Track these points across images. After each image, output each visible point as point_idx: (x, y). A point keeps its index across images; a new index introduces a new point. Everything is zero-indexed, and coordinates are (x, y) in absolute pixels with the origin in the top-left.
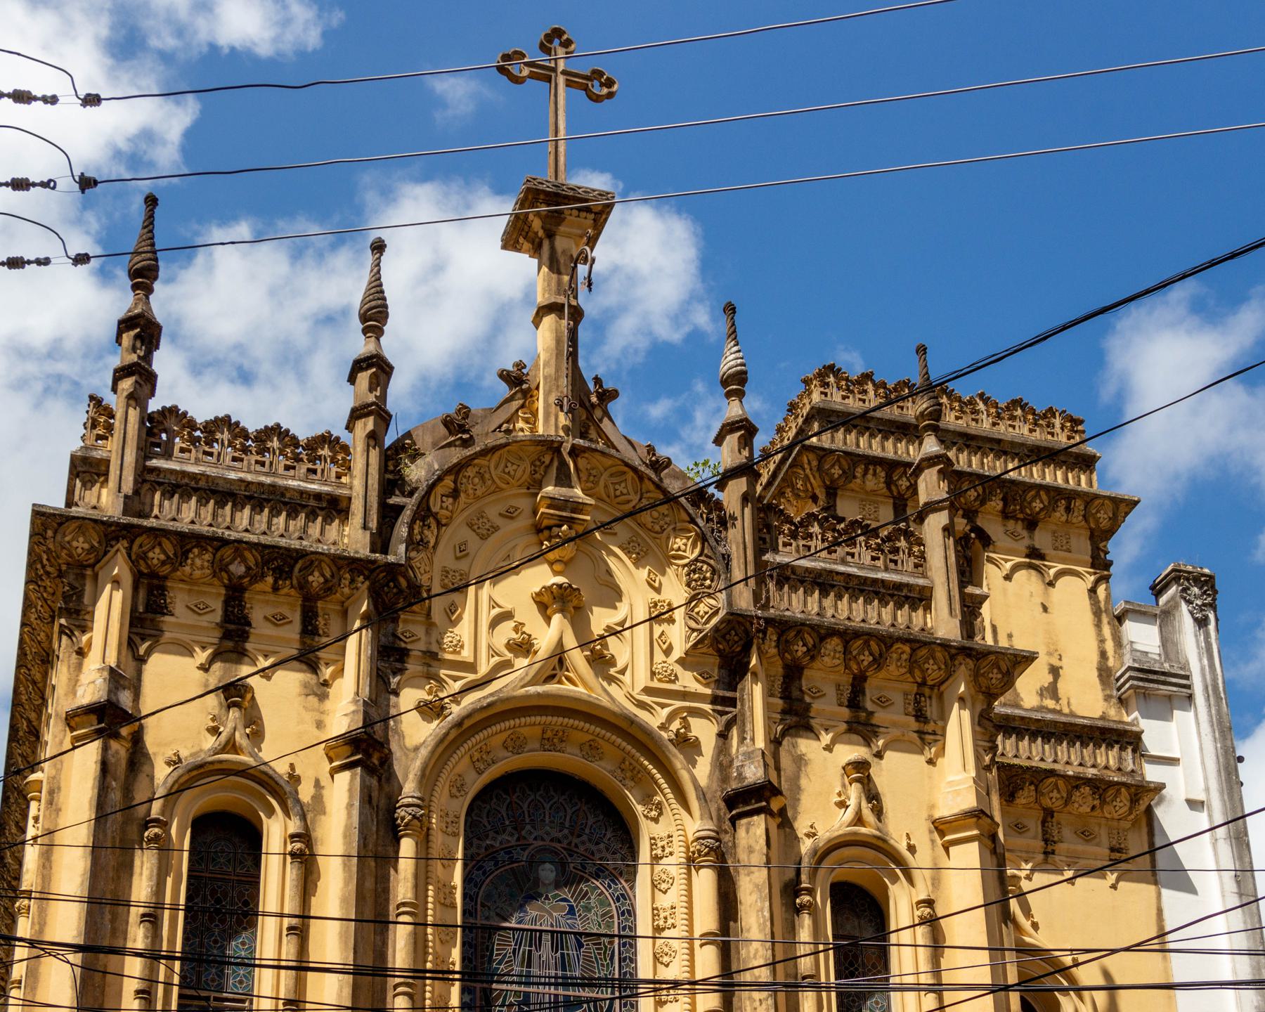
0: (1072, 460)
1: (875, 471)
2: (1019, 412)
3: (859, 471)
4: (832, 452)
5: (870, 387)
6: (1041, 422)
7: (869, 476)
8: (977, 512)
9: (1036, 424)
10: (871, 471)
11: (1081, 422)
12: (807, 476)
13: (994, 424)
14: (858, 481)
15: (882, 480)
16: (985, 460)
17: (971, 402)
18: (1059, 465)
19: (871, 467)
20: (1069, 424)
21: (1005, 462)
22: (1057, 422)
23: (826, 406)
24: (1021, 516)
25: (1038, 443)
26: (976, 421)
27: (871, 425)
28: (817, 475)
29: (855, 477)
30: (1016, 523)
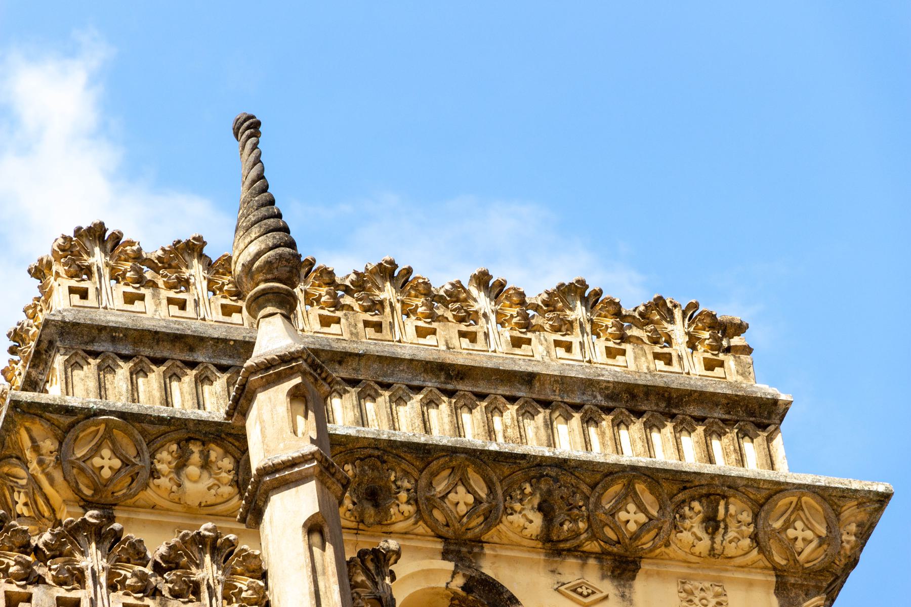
0: (719, 414)
1: (205, 456)
2: (579, 312)
3: (165, 459)
4: (89, 414)
5: (196, 271)
6: (635, 332)
7: (193, 470)
8: (479, 542)
9: (624, 338)
10: (196, 457)
11: (740, 328)
12: (33, 479)
13: (517, 343)
14: (163, 481)
15: (226, 477)
16: (497, 422)
17: (456, 294)
18: (685, 425)
19: (195, 448)
20: (706, 334)
21: (549, 425)
22: (678, 330)
23: (83, 317)
24: (593, 546)
25: (630, 379)
26: (472, 337)
27: (200, 357)
28: (58, 475)
29: (154, 474)
30: (583, 565)
